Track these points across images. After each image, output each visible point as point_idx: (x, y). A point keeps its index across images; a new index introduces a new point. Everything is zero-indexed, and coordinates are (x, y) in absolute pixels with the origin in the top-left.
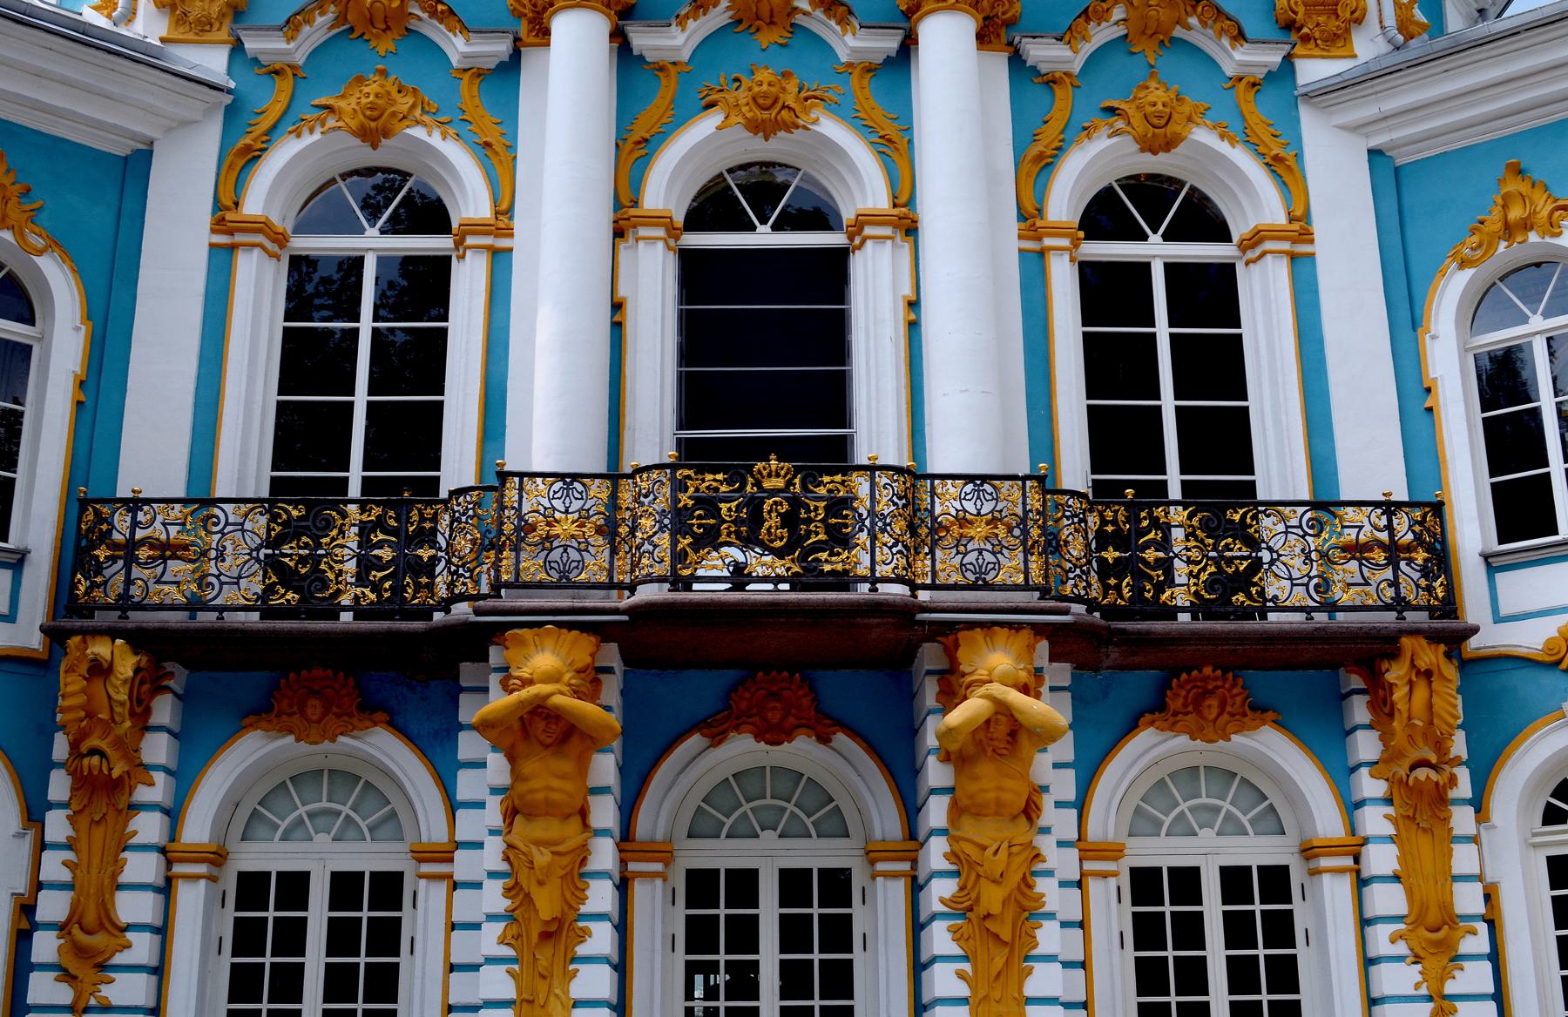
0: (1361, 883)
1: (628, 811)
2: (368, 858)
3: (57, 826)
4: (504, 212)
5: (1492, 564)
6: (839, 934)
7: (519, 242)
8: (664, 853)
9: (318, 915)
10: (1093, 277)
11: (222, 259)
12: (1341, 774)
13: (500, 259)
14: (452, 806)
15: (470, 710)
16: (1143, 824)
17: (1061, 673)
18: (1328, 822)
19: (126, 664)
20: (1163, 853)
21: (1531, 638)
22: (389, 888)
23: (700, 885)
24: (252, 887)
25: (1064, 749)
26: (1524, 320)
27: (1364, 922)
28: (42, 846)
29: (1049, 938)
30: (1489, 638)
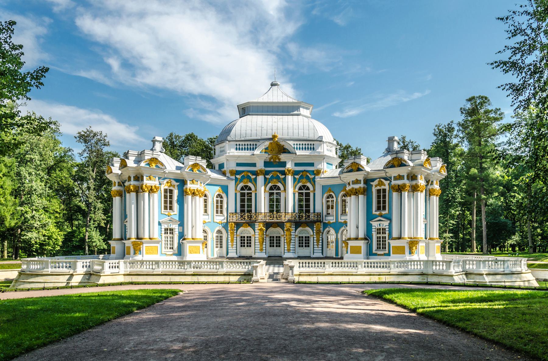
0: (314, 238)
1: (266, 232)
2: (249, 235)
3: (229, 234)
4: (256, 190)
5: (326, 216)
6: (279, 240)
7: (257, 192)
8: (268, 235)
9: (246, 239)
10: (299, 193)
11: (236, 194)
12: (313, 231)
13: (256, 194)
14: (255, 232)
15: (256, 226)
16: (300, 233)
17: (294, 224)
18: (312, 233)
19: (234, 224)
20: (301, 235)
21: (327, 222)
22: (250, 237)
23: (270, 237)
24: (241, 237)
25: (294, 229)
26: (329, 198)
27: (314, 240)
28: (228, 235)
29: (292, 241)
30: (324, 221)
